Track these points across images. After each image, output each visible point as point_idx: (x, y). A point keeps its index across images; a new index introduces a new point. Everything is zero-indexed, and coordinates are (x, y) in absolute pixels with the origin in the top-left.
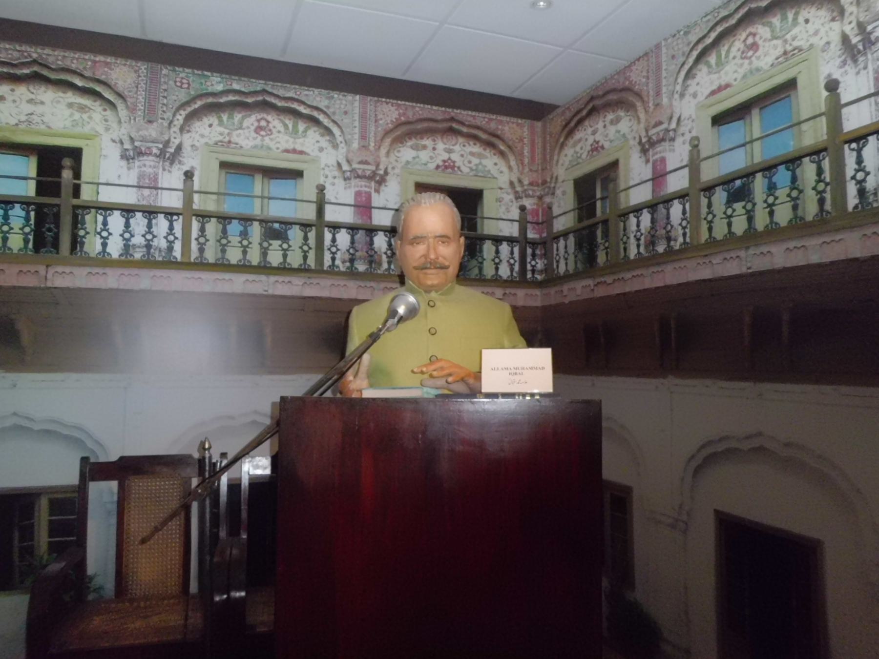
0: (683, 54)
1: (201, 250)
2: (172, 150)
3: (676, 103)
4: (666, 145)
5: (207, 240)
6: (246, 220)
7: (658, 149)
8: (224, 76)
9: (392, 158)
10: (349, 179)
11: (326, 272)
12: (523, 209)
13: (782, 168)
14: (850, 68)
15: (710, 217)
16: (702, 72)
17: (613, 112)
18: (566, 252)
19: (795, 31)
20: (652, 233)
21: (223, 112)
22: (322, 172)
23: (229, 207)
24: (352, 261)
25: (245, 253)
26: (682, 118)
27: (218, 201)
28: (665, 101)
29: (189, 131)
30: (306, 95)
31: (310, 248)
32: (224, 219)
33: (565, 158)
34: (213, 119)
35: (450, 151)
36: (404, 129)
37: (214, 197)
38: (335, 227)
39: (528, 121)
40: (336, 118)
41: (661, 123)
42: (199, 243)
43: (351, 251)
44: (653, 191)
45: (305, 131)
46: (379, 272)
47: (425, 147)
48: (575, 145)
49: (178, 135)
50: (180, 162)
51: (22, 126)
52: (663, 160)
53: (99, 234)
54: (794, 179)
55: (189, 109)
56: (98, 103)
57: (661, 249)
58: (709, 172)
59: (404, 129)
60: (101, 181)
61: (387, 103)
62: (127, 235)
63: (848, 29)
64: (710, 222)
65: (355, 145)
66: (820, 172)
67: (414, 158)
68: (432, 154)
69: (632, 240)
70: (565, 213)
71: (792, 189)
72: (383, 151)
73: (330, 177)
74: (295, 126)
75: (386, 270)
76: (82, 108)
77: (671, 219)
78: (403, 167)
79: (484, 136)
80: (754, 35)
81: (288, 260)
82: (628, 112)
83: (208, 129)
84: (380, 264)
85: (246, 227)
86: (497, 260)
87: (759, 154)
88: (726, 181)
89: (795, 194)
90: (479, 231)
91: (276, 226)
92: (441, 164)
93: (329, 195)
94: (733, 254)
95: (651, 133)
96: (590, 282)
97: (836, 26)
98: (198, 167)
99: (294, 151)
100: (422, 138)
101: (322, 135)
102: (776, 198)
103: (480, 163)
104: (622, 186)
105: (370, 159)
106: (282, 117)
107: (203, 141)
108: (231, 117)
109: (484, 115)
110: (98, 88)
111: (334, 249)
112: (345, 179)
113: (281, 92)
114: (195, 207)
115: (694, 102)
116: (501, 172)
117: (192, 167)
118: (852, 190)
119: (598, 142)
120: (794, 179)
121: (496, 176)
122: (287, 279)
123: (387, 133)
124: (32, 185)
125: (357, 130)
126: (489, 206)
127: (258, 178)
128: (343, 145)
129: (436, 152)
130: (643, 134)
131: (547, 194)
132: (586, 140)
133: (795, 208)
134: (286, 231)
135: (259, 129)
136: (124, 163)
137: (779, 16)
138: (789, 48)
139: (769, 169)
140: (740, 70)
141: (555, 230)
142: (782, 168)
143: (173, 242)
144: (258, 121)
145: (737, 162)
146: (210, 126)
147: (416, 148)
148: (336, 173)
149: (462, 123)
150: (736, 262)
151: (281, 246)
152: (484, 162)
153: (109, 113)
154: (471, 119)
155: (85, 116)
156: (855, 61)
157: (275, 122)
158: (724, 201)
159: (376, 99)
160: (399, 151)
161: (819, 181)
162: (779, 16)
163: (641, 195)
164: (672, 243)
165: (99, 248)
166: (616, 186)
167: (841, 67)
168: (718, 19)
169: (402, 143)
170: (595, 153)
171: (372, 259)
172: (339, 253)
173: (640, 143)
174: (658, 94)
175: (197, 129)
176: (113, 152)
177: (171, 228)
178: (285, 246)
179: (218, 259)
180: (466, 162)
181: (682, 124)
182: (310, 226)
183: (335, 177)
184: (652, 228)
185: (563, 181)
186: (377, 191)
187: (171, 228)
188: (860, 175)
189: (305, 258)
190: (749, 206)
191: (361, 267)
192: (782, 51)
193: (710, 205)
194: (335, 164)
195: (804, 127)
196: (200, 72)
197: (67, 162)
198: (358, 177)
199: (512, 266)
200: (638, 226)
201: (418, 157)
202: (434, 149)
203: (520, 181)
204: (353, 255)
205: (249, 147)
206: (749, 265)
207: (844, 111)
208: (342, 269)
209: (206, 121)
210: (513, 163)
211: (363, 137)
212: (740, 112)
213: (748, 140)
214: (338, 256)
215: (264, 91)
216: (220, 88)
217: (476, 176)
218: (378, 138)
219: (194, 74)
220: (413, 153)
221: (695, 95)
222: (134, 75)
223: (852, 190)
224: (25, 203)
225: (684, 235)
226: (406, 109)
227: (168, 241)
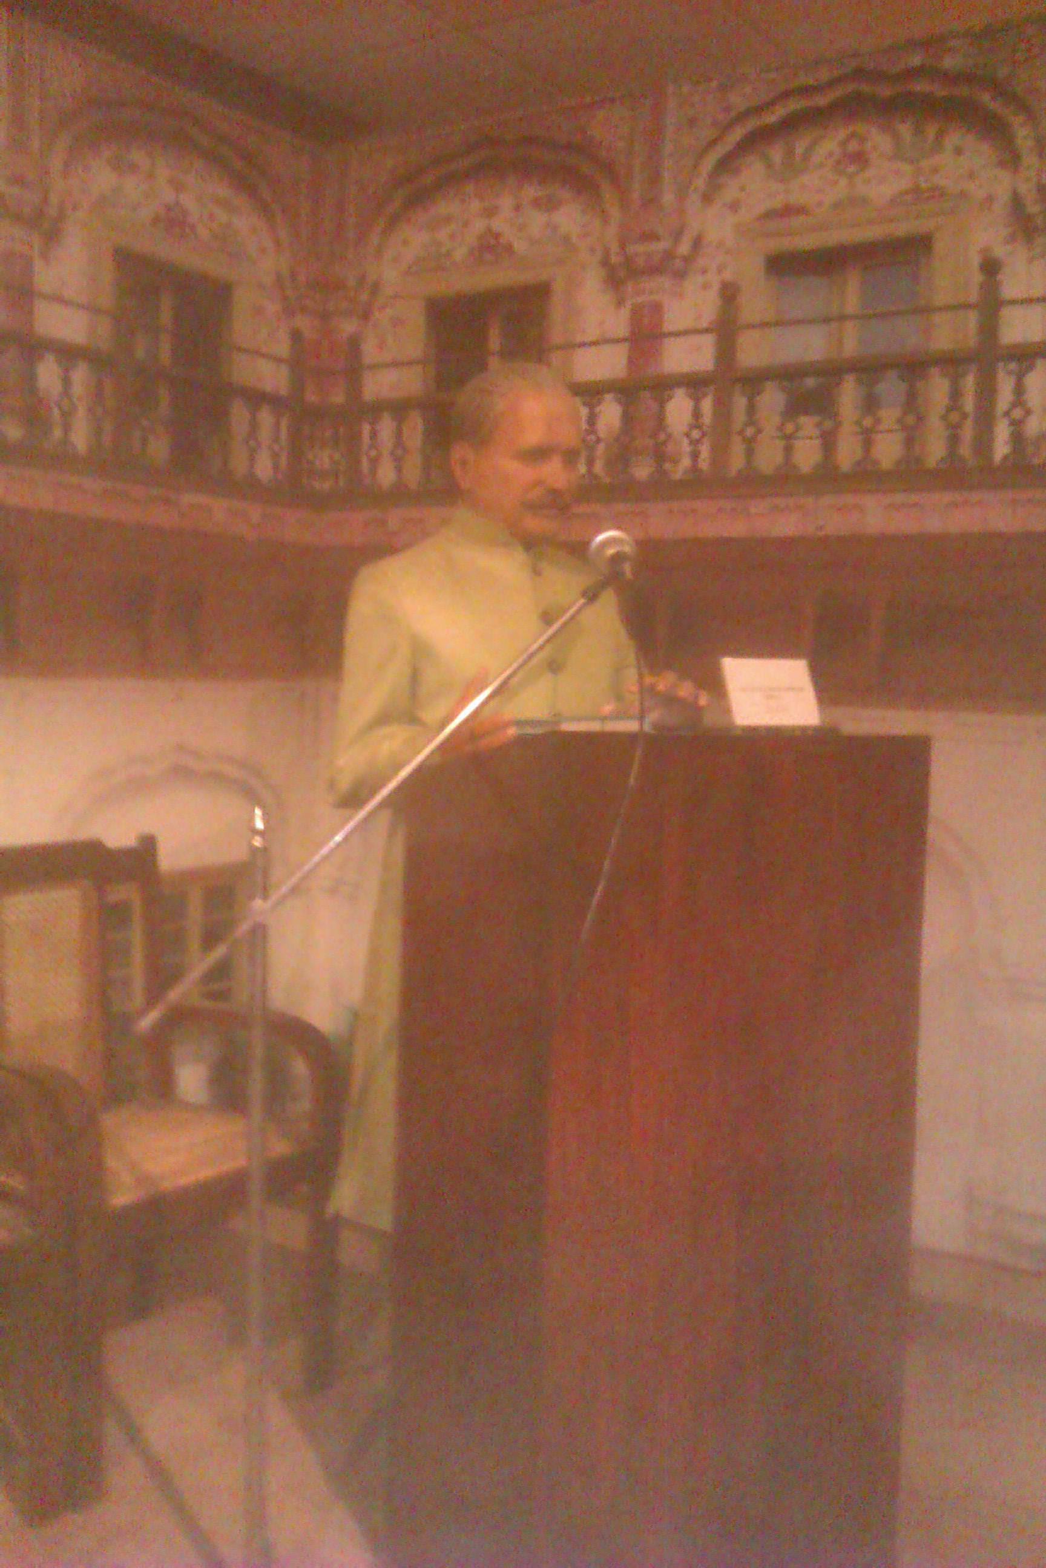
0: (715, 123)
4: (664, 282)
12: (296, 336)
28: (668, 198)
35: (178, 187)
47: (133, 168)
52: (657, 308)
57: (642, 471)
58: (753, 352)
63: (1023, 189)
66: (956, 394)
72: (56, 164)
80: (862, 140)
82: (579, 193)
87: (851, 345)
95: (631, 249)
97: (1005, 176)
118: (1002, 432)
119: (497, 236)
130: (615, 247)
132: (466, 224)
133: (909, 442)
139: (869, 369)
145: (809, 345)
147: (119, 166)
161: (950, 409)
164: (667, 466)
167: (1006, 243)
170: (488, 257)
173: (605, 263)
174: (655, 179)
186: (45, 256)
188: (1017, 414)
190: (828, 424)
193: (751, 409)
195: (938, 318)
199: (275, 456)
207: (1006, 312)
212: (828, 262)
223: (1002, 432)
225: (695, 456)
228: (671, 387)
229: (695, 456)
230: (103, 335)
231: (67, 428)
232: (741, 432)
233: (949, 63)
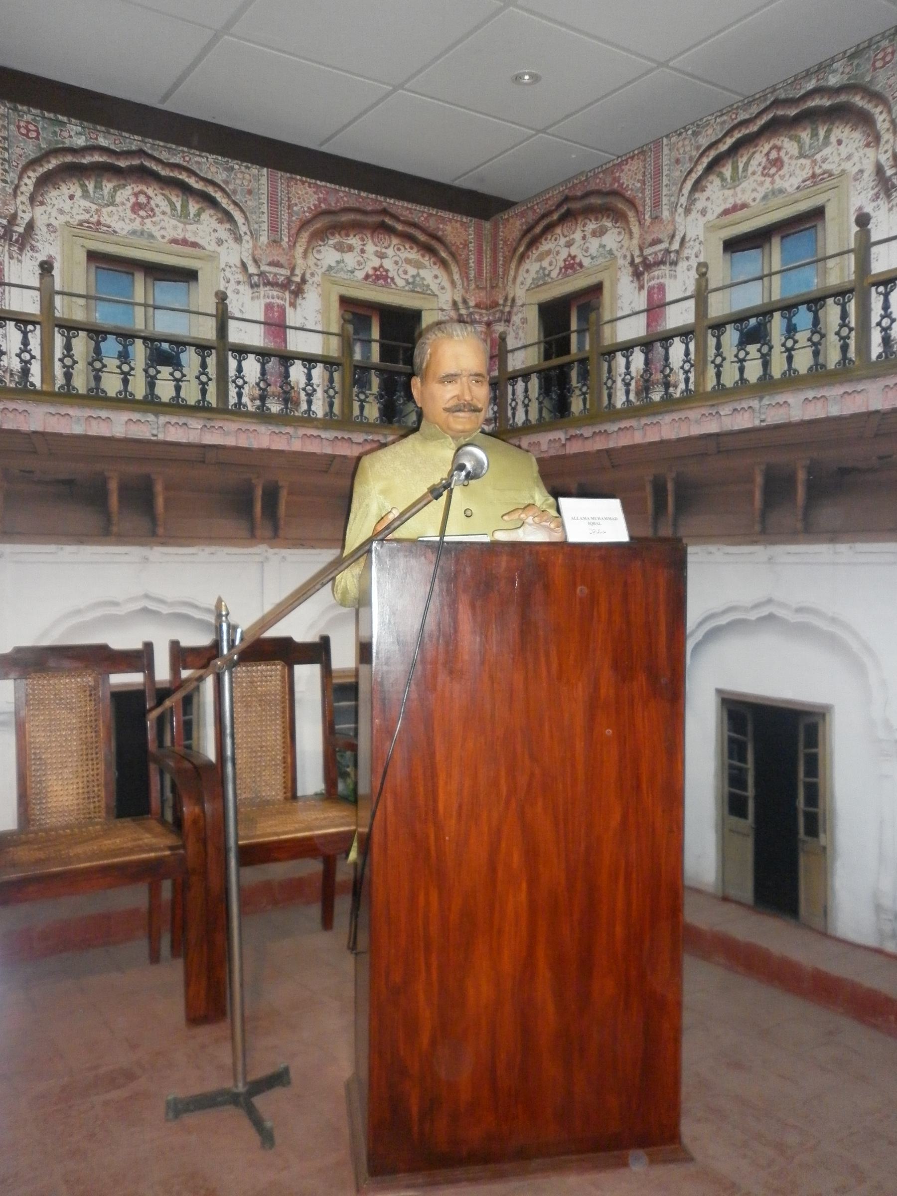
0: (691, 159)
1: (68, 376)
2: (21, 230)
3: (679, 219)
4: (665, 269)
5: (75, 362)
6: (126, 336)
7: (656, 273)
8: (86, 124)
9: (311, 261)
10: (258, 286)
13: (803, 308)
14: (882, 203)
15: (718, 360)
16: (713, 185)
17: (596, 219)
18: (526, 397)
19: (826, 151)
20: (646, 377)
22: (222, 274)
23: (103, 316)
24: (263, 398)
25: (126, 382)
26: (687, 239)
27: (87, 307)
28: (666, 214)
29: (42, 203)
30: (198, 163)
31: (210, 379)
32: (97, 334)
33: (525, 275)
34: (71, 188)
35: (382, 256)
37: (82, 301)
38: (242, 351)
39: (474, 220)
40: (238, 198)
41: (659, 241)
42: (64, 366)
43: (262, 385)
44: (648, 325)
45: (198, 215)
46: (296, 414)
47: (351, 248)
48: (540, 259)
50: (33, 248)
52: (661, 288)
54: (816, 321)
55: (41, 170)
57: (656, 396)
58: (718, 307)
61: (303, 183)
64: (718, 367)
65: (264, 239)
66: (844, 315)
67: (338, 262)
68: (360, 258)
69: (619, 384)
70: (525, 347)
71: (813, 333)
72: (299, 250)
73: (232, 282)
74: (185, 206)
75: (305, 412)
77: (670, 360)
78: (324, 274)
79: (422, 238)
80: (779, 149)
81: (183, 394)
84: (297, 404)
85: (125, 347)
87: (778, 291)
88: (739, 319)
89: (816, 338)
91: (165, 346)
92: (371, 272)
93: (233, 307)
94: (745, 404)
96: (560, 435)
97: (870, 152)
98: (58, 257)
99: (185, 242)
100: (348, 235)
101: (220, 222)
102: (796, 342)
103: (418, 274)
104: (607, 317)
105: (283, 260)
106: (167, 192)
107: (63, 219)
109: (422, 208)
111: (240, 382)
112: (252, 286)
113: (164, 156)
114: (57, 314)
115: (702, 221)
116: (443, 288)
117: (50, 256)
118: (876, 337)
119: (574, 258)
120: (816, 321)
123: (304, 225)
125: (265, 218)
127: (139, 280)
128: (247, 238)
129: (365, 255)
130: (637, 253)
131: (500, 320)
132: (558, 253)
133: (816, 354)
134: (178, 354)
135: (137, 207)
137: (809, 131)
138: (818, 171)
139: (788, 308)
140: (759, 189)
141: (510, 369)
142: (803, 308)
143: (29, 362)
144: (136, 195)
145: (750, 297)
146: (71, 197)
147: (340, 248)
148: (240, 277)
150: (747, 415)
152: (422, 273)
156: (888, 196)
157: (158, 198)
158: (736, 342)
159: (288, 175)
160: (319, 252)
161: (842, 326)
162: (809, 131)
163: (632, 329)
164: (671, 390)
166: (599, 317)
167: (873, 201)
168: (736, 122)
170: (570, 271)
171: (288, 397)
172: (246, 386)
173: (632, 263)
174: (657, 204)
175: (54, 201)
177: (25, 342)
178: (178, 375)
179: (91, 390)
180: (400, 272)
181: (687, 245)
182: (210, 348)
183: (239, 283)
184: (645, 371)
185: (522, 306)
186: (293, 305)
187: (25, 342)
189: (204, 392)
190: (765, 349)
191: (275, 407)
192: (810, 174)
193: (718, 346)
194: (239, 264)
195: (831, 263)
196: (52, 116)
198: (268, 283)
200: (628, 367)
201: (343, 261)
203: (465, 301)
204: (264, 390)
205: (125, 232)
206: (763, 417)
207: (874, 250)
208: (251, 408)
210: (456, 277)
211: (274, 228)
213: (766, 272)
214: (246, 391)
215: (141, 153)
216: (81, 142)
217: (413, 291)
218: (293, 231)
219: (44, 118)
220: (337, 256)
221: (704, 212)
223: (876, 337)
225: (687, 380)
226: (327, 193)
227: (22, 361)
228: (671, 337)
229: (687, 380)
230: (334, 348)
231: (310, 402)
232: (713, 362)
233: (833, 80)
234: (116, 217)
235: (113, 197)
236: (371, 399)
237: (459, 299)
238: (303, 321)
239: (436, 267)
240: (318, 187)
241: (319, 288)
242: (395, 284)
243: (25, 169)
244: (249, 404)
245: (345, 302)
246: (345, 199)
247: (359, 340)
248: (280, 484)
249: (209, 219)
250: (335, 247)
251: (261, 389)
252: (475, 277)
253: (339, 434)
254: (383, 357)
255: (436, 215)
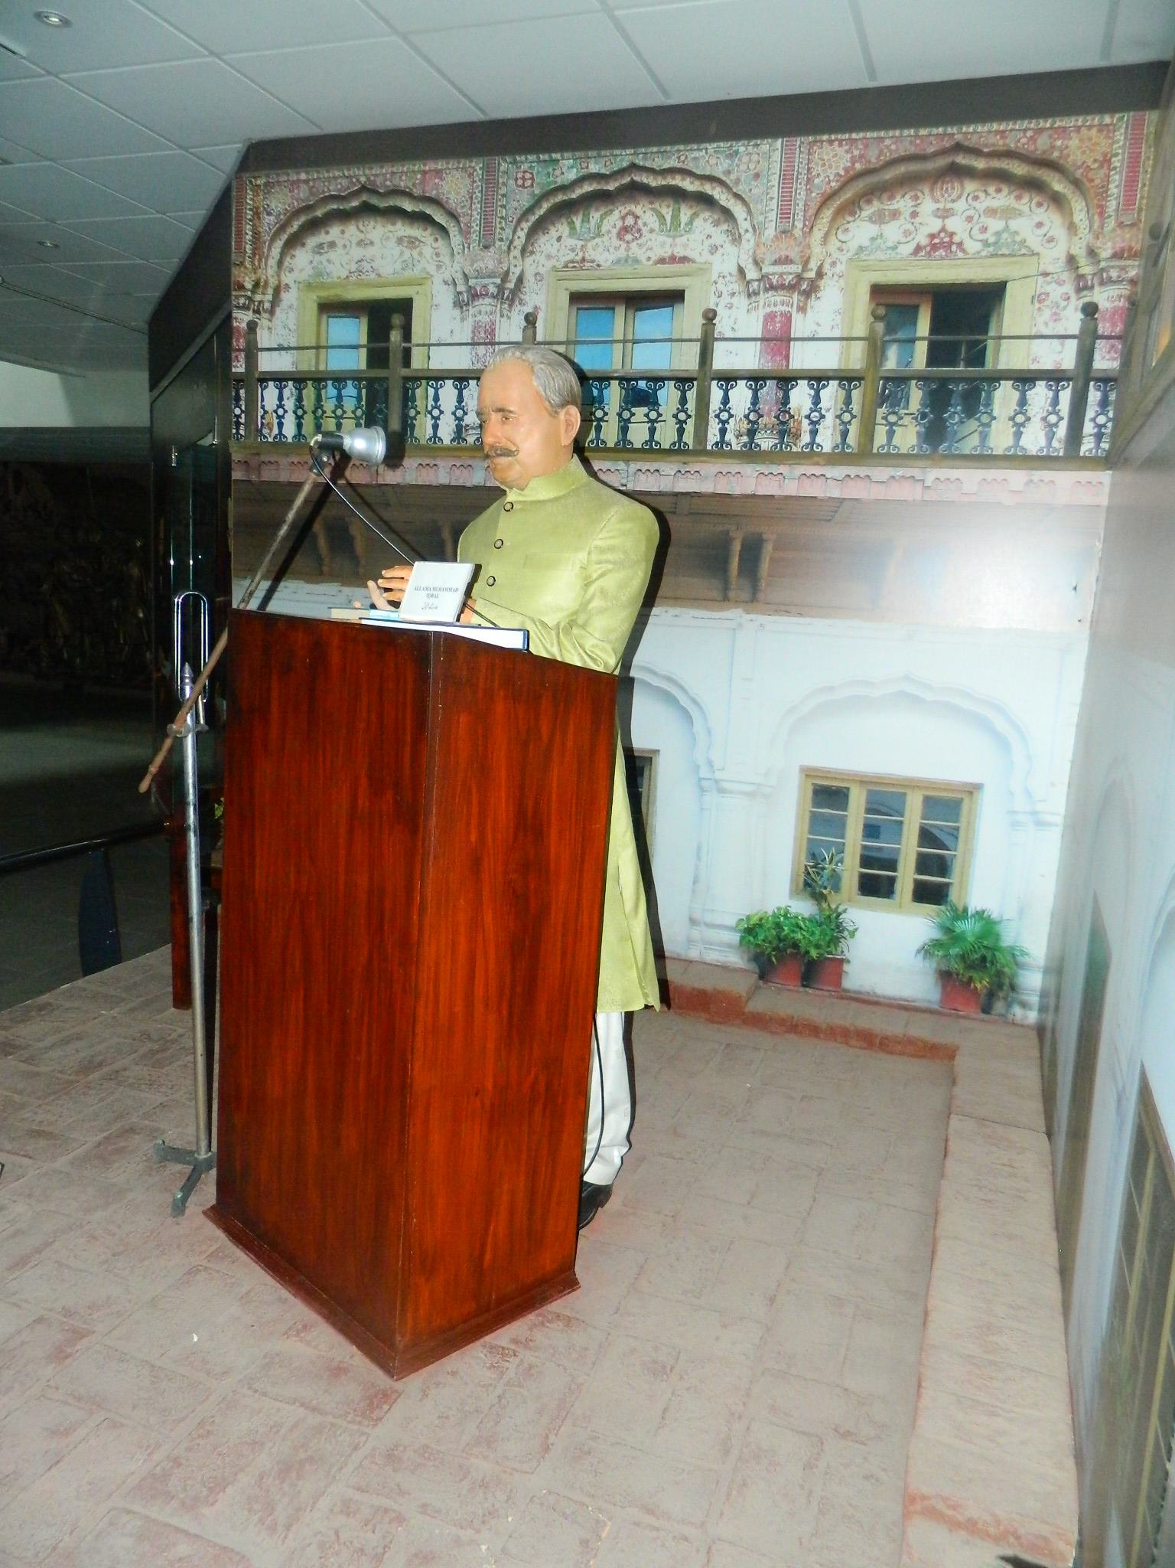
2: (511, 285)
8: (578, 154)
9: (834, 243)
10: (756, 294)
11: (710, 454)
12: (1090, 310)
21: (576, 213)
24: (751, 433)
29: (532, 253)
30: (695, 159)
31: (689, 417)
34: (561, 228)
36: (860, 185)
38: (728, 379)
39: (1128, 116)
40: (739, 189)
45: (690, 222)
46: (794, 449)
47: (895, 215)
49: (519, 262)
51: (353, 278)
53: (430, 413)
55: (533, 218)
56: (429, 230)
59: (860, 185)
60: (433, 341)
61: (831, 142)
62: (459, 413)
65: (770, 232)
67: (873, 239)
74: (675, 217)
76: (412, 242)
79: (1019, 169)
81: (657, 437)
83: (556, 245)
84: (797, 436)
86: (1020, 419)
90: (989, 364)
91: (642, 384)
92: (924, 241)
93: (722, 326)
98: (543, 307)
99: (673, 259)
100: (891, 198)
105: (794, 254)
106: (657, 205)
107: (549, 264)
108: (586, 219)
109: (1025, 124)
110: (429, 210)
111: (724, 416)
112: (749, 296)
113: (659, 163)
116: (1051, 240)
121: (1037, 248)
122: (653, 466)
124: (363, 353)
125: (774, 204)
126: (1015, 314)
128: (749, 235)
129: (917, 220)
136: (457, 312)
146: (559, 239)
147: (879, 219)
148: (736, 287)
149: (976, 152)
151: (647, 415)
152: (1014, 224)
153: (441, 242)
154: (992, 139)
155: (415, 253)
157: (645, 212)
160: (847, 230)
165: (430, 432)
169: (853, 213)
171: (785, 430)
176: (444, 297)
178: (653, 415)
180: (975, 231)
182: (691, 380)
186: (802, 309)
189: (681, 432)
194: (735, 271)
197: (397, 320)
198: (772, 288)
199: (1050, 429)
202: (914, 215)
203: (1092, 253)
208: (736, 447)
209: (553, 232)
211: (785, 214)
215: (634, 167)
216: (572, 175)
218: (811, 212)
219: (539, 161)
220: (873, 229)
222: (468, 181)
224: (356, 377)
226: (866, 146)
230: (856, 358)
231: (814, 433)
234: (601, 249)
235: (599, 227)
236: (907, 420)
237: (1079, 251)
238: (815, 327)
239: (1042, 210)
240: (841, 142)
241: (842, 281)
242: (964, 251)
243: (519, 221)
244: (734, 441)
245: (878, 291)
246: (893, 147)
247: (895, 341)
248: (765, 536)
249: (704, 224)
250: (870, 219)
251: (750, 421)
252: (1117, 210)
253: (852, 471)
254: (933, 359)
255: (1051, 128)
